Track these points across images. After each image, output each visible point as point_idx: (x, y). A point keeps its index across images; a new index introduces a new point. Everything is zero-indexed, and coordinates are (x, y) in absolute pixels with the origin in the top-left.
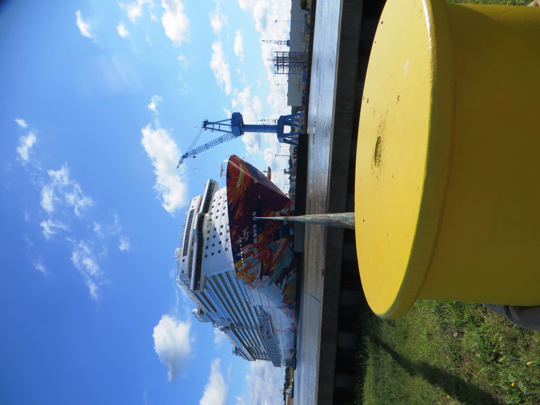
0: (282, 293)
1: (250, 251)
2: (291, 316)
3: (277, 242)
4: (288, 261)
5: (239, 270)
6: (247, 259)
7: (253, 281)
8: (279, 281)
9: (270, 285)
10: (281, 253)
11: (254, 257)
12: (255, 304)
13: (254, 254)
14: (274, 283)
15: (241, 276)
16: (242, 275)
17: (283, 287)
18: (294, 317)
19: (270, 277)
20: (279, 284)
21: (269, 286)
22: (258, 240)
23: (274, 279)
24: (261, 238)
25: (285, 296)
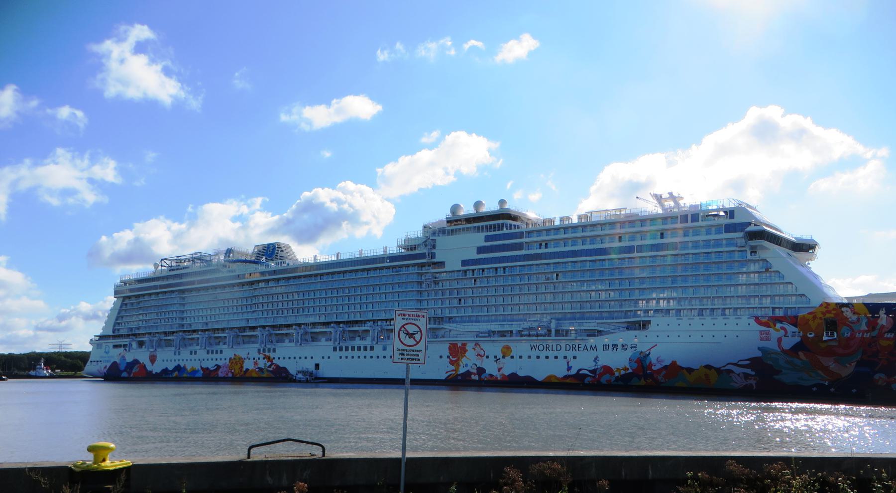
0: (708, 367)
1: (878, 327)
2: (579, 376)
3: (854, 364)
4: (787, 377)
5: (844, 309)
6: (864, 321)
7: (795, 325)
8: (754, 363)
9: (759, 349)
10: (826, 369)
11: (859, 332)
12: (654, 321)
13: (867, 331)
14: (759, 354)
15: (824, 310)
16: (829, 312)
17: (730, 367)
18: (568, 381)
19: (784, 352)
20: (748, 362)
21: (759, 349)
22: (888, 339)
23: (773, 356)
24: (884, 343)
25: (690, 370)
